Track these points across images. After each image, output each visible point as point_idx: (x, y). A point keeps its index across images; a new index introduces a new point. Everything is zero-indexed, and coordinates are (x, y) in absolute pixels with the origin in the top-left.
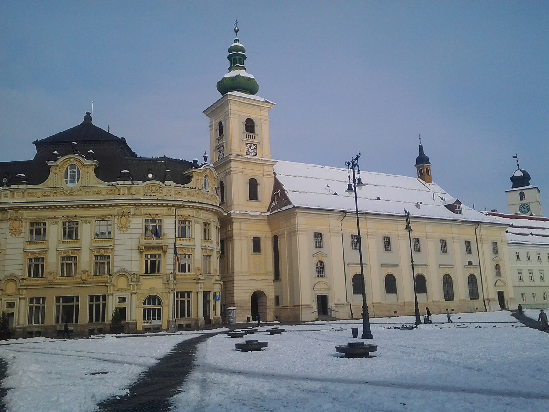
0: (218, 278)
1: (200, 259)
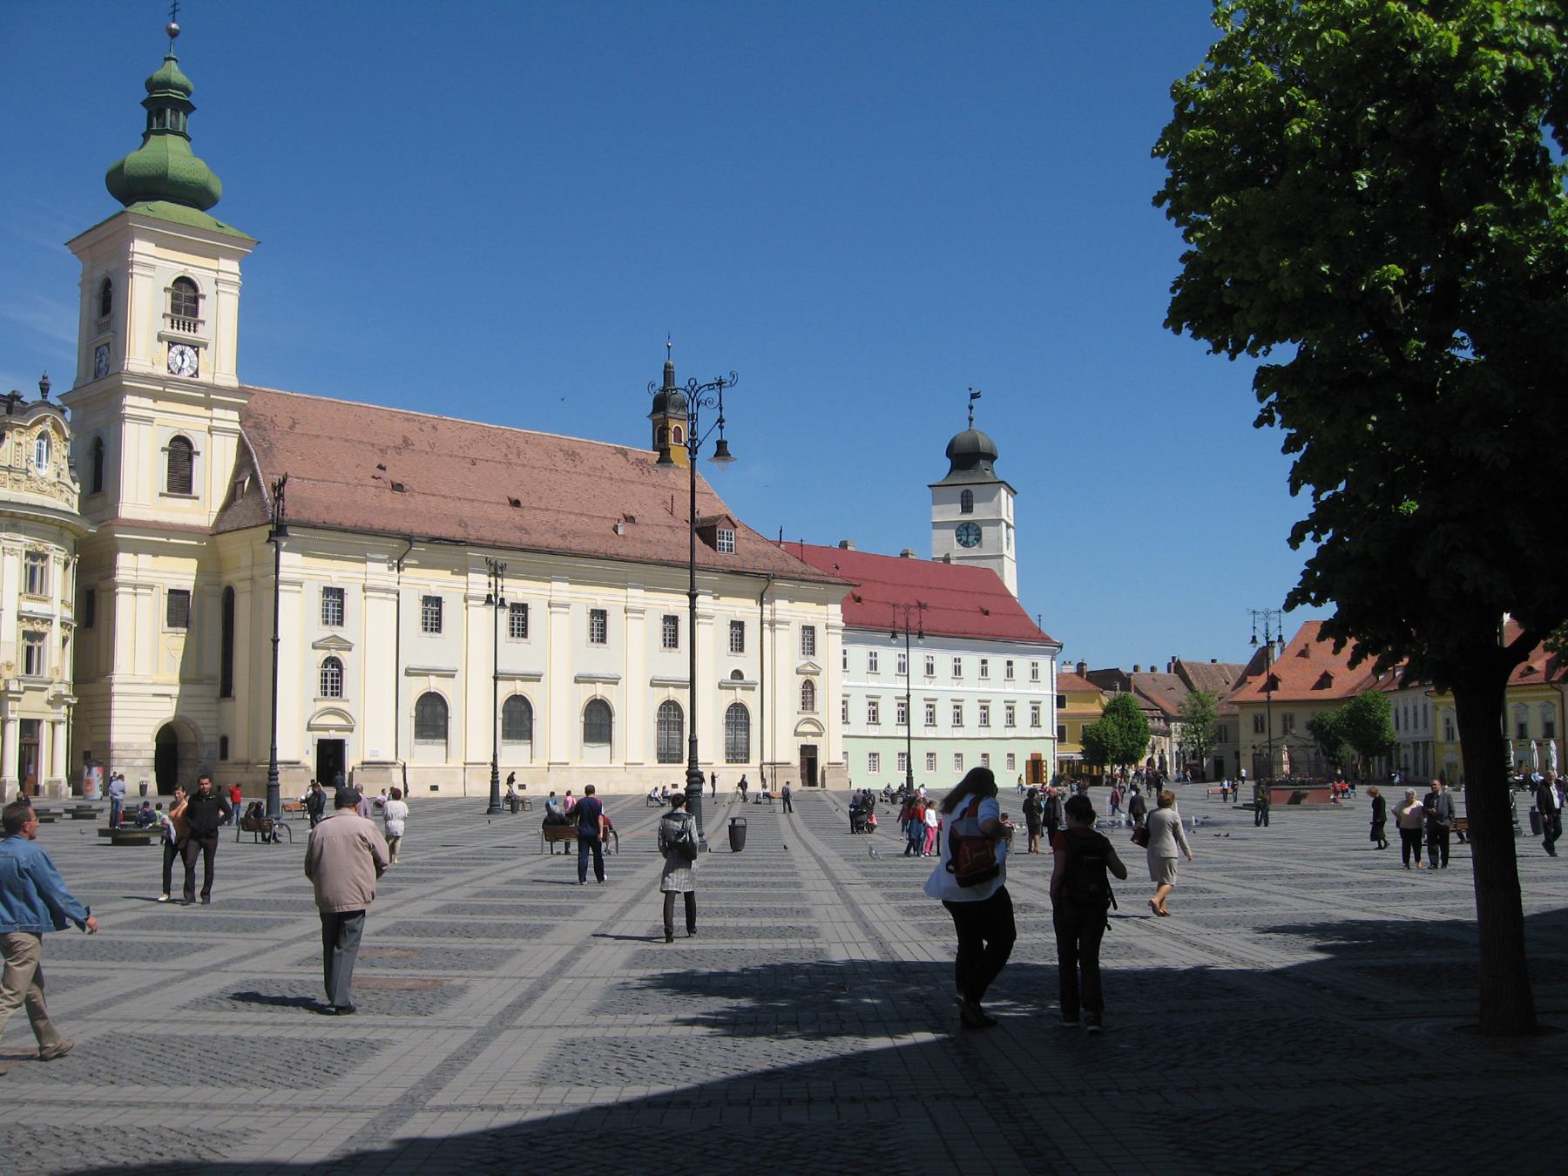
0: (65, 690)
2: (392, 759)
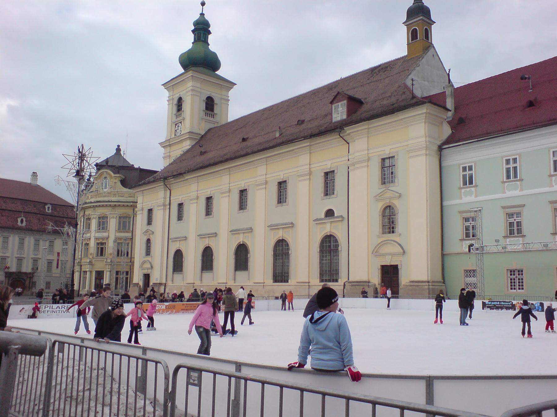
1: (93, 246)
2: (164, 281)
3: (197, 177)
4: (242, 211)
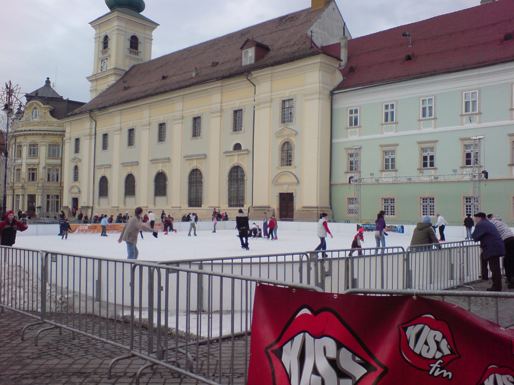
2: (91, 205)
3: (121, 110)
4: (161, 142)
